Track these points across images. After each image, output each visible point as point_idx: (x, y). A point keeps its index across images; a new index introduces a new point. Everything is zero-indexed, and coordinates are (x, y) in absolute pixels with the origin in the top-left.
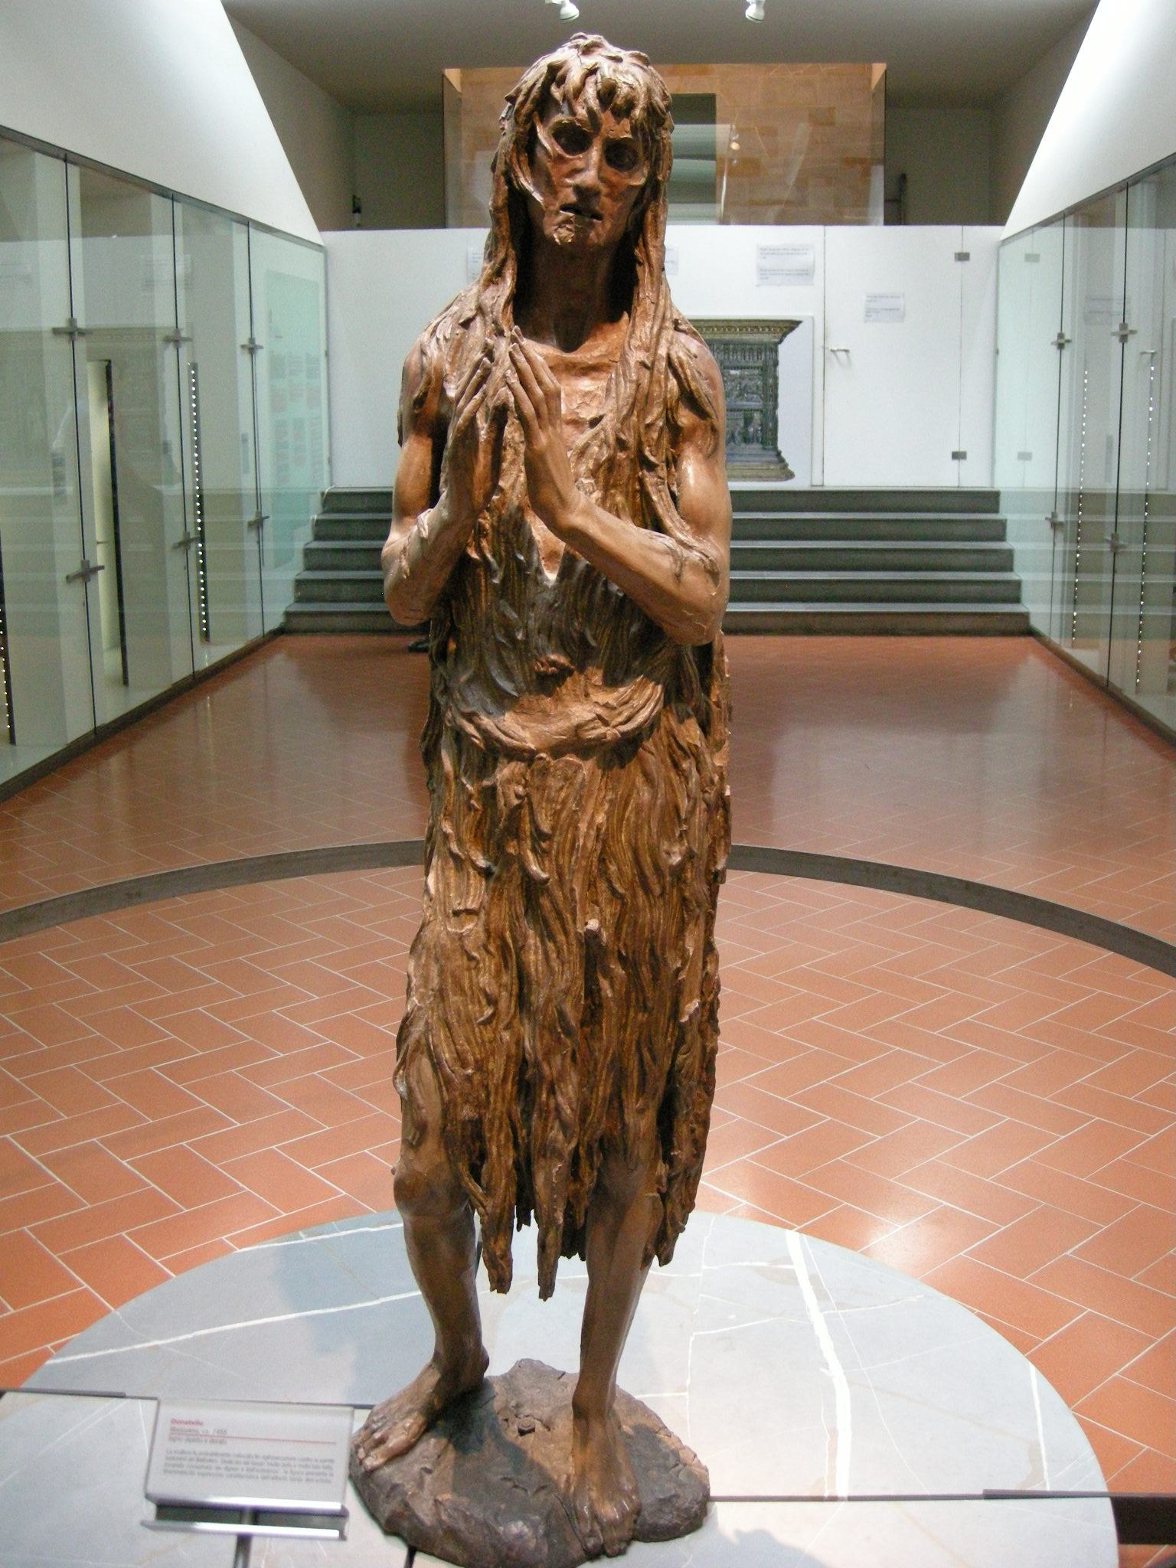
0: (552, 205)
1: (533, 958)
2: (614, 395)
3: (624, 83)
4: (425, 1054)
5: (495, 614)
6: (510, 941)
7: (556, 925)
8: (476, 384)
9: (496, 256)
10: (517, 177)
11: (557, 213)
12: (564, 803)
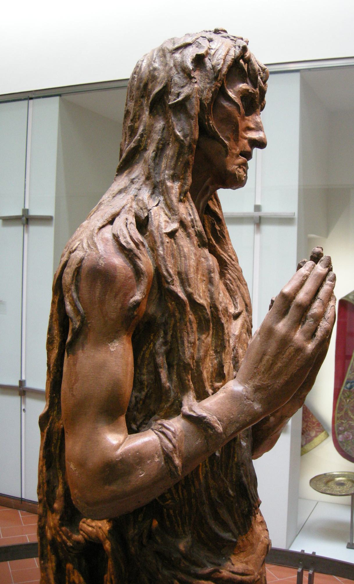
0: (235, 149)
2: (239, 294)
5: (211, 482)
9: (184, 179)
10: (209, 120)
11: (237, 156)
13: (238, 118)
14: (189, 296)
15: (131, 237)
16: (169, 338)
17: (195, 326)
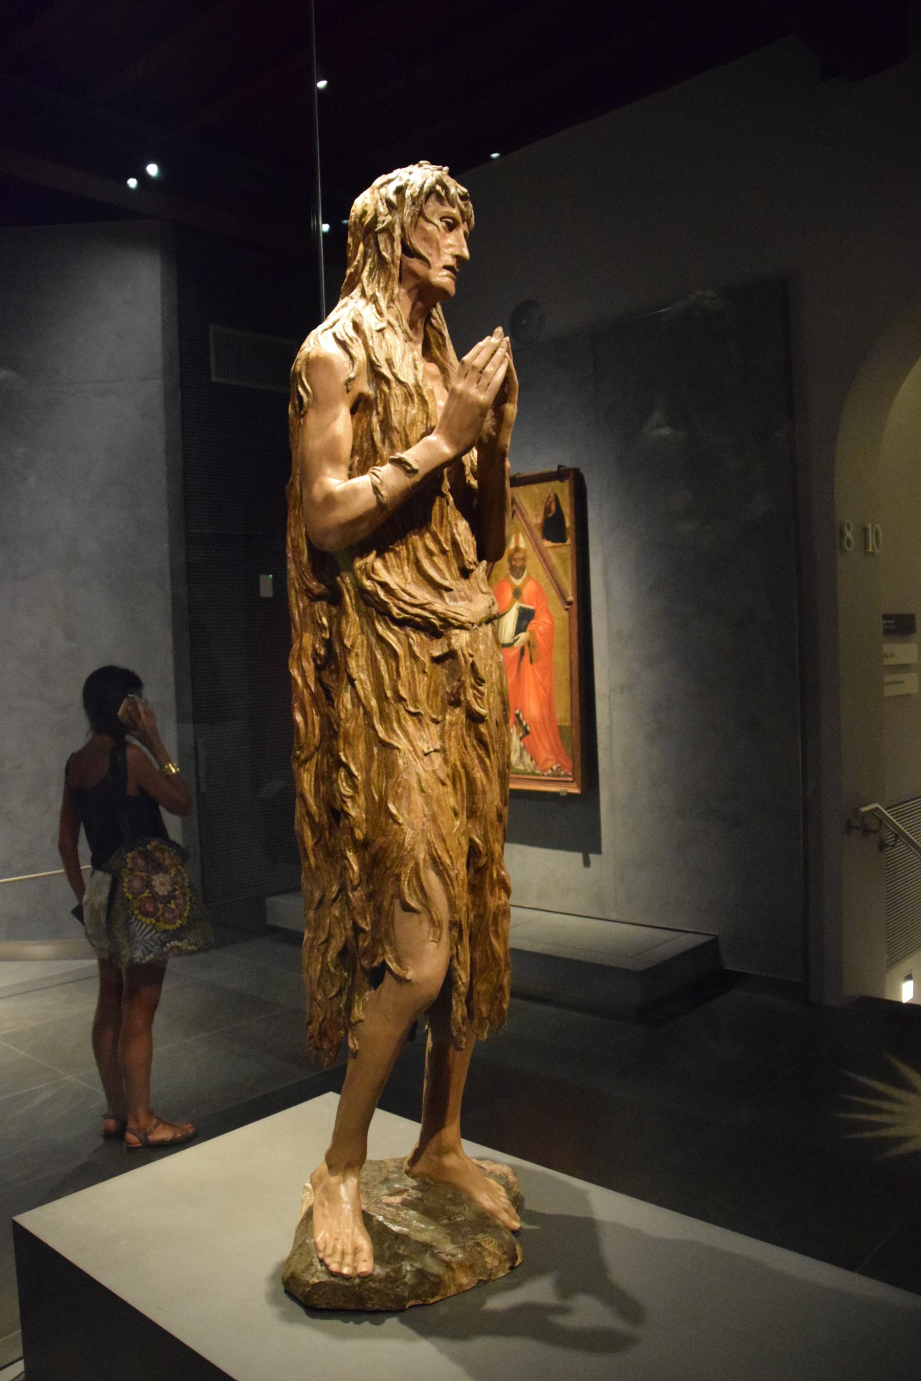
0: (437, 263)
1: (479, 774)
4: (430, 868)
6: (460, 768)
7: (490, 748)
11: (440, 269)
12: (486, 660)
13: (438, 237)
14: (394, 375)
15: (346, 334)
16: (380, 409)
17: (400, 399)
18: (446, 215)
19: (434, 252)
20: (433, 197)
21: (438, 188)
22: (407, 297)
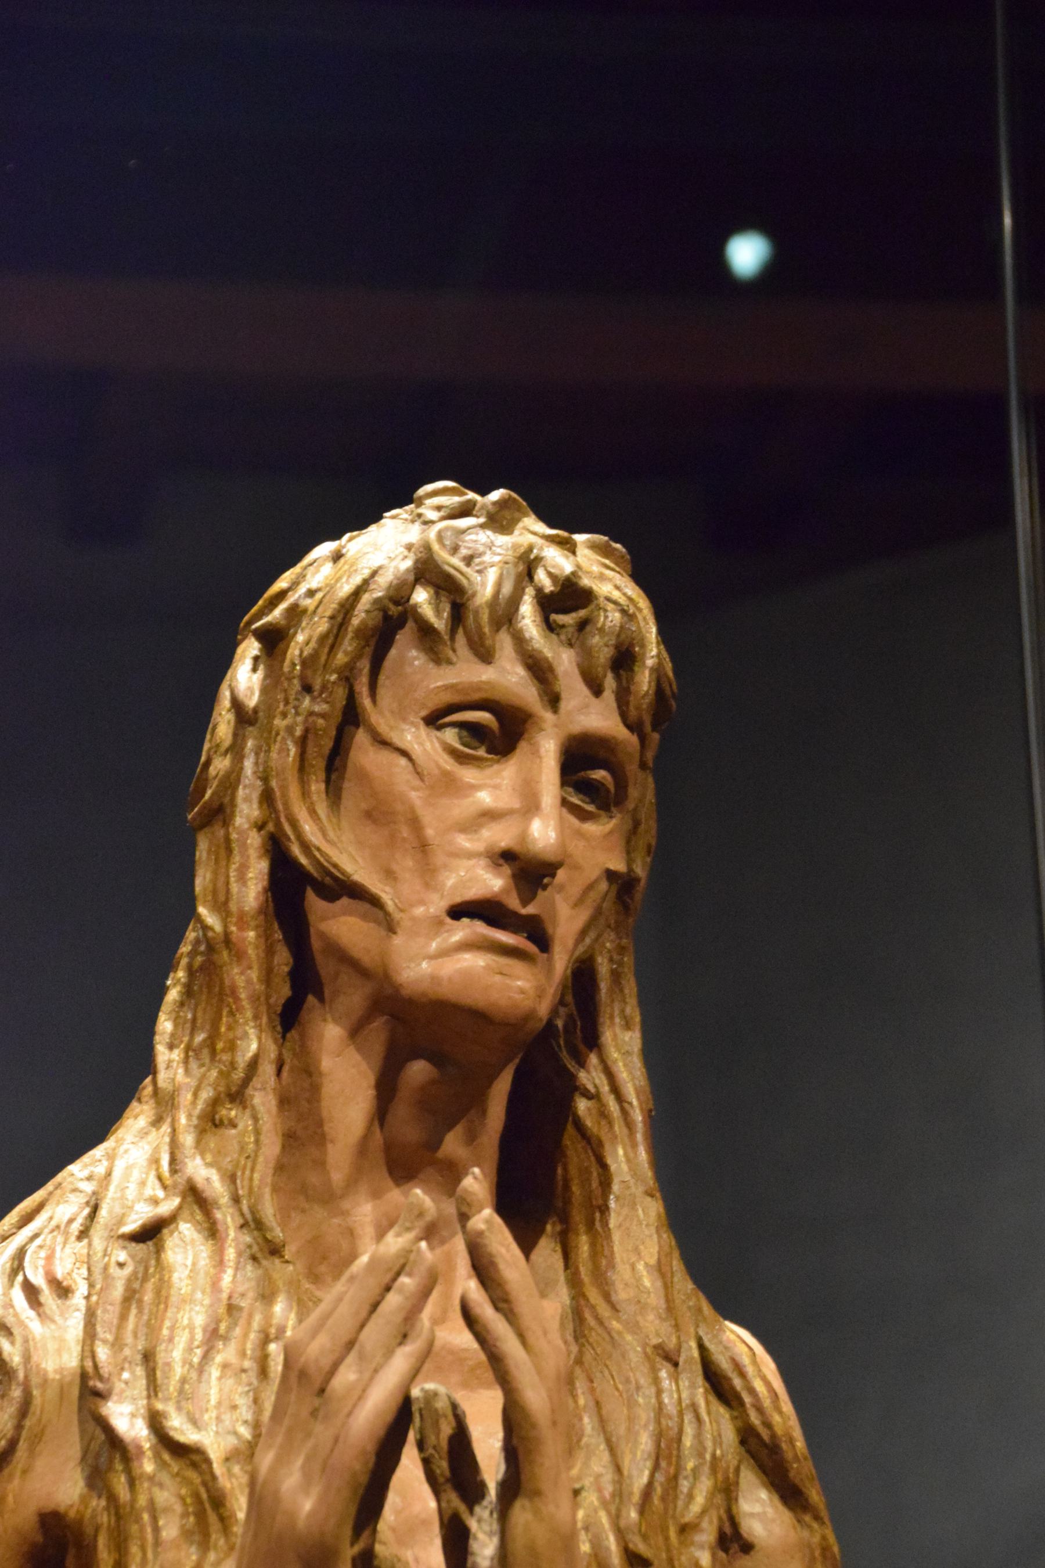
0: (422, 902)
3: (608, 599)
8: (398, 1318)
9: (232, 1047)
13: (415, 797)
18: (447, 698)
19: (406, 863)
20: (404, 638)
21: (421, 596)
22: (353, 1055)
